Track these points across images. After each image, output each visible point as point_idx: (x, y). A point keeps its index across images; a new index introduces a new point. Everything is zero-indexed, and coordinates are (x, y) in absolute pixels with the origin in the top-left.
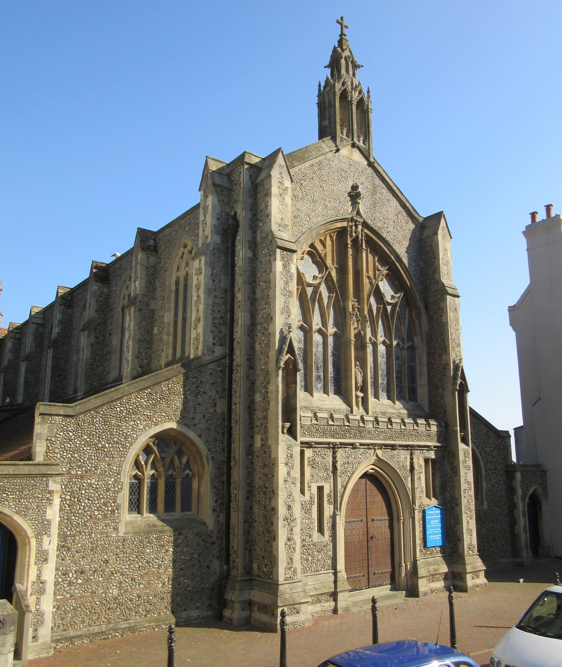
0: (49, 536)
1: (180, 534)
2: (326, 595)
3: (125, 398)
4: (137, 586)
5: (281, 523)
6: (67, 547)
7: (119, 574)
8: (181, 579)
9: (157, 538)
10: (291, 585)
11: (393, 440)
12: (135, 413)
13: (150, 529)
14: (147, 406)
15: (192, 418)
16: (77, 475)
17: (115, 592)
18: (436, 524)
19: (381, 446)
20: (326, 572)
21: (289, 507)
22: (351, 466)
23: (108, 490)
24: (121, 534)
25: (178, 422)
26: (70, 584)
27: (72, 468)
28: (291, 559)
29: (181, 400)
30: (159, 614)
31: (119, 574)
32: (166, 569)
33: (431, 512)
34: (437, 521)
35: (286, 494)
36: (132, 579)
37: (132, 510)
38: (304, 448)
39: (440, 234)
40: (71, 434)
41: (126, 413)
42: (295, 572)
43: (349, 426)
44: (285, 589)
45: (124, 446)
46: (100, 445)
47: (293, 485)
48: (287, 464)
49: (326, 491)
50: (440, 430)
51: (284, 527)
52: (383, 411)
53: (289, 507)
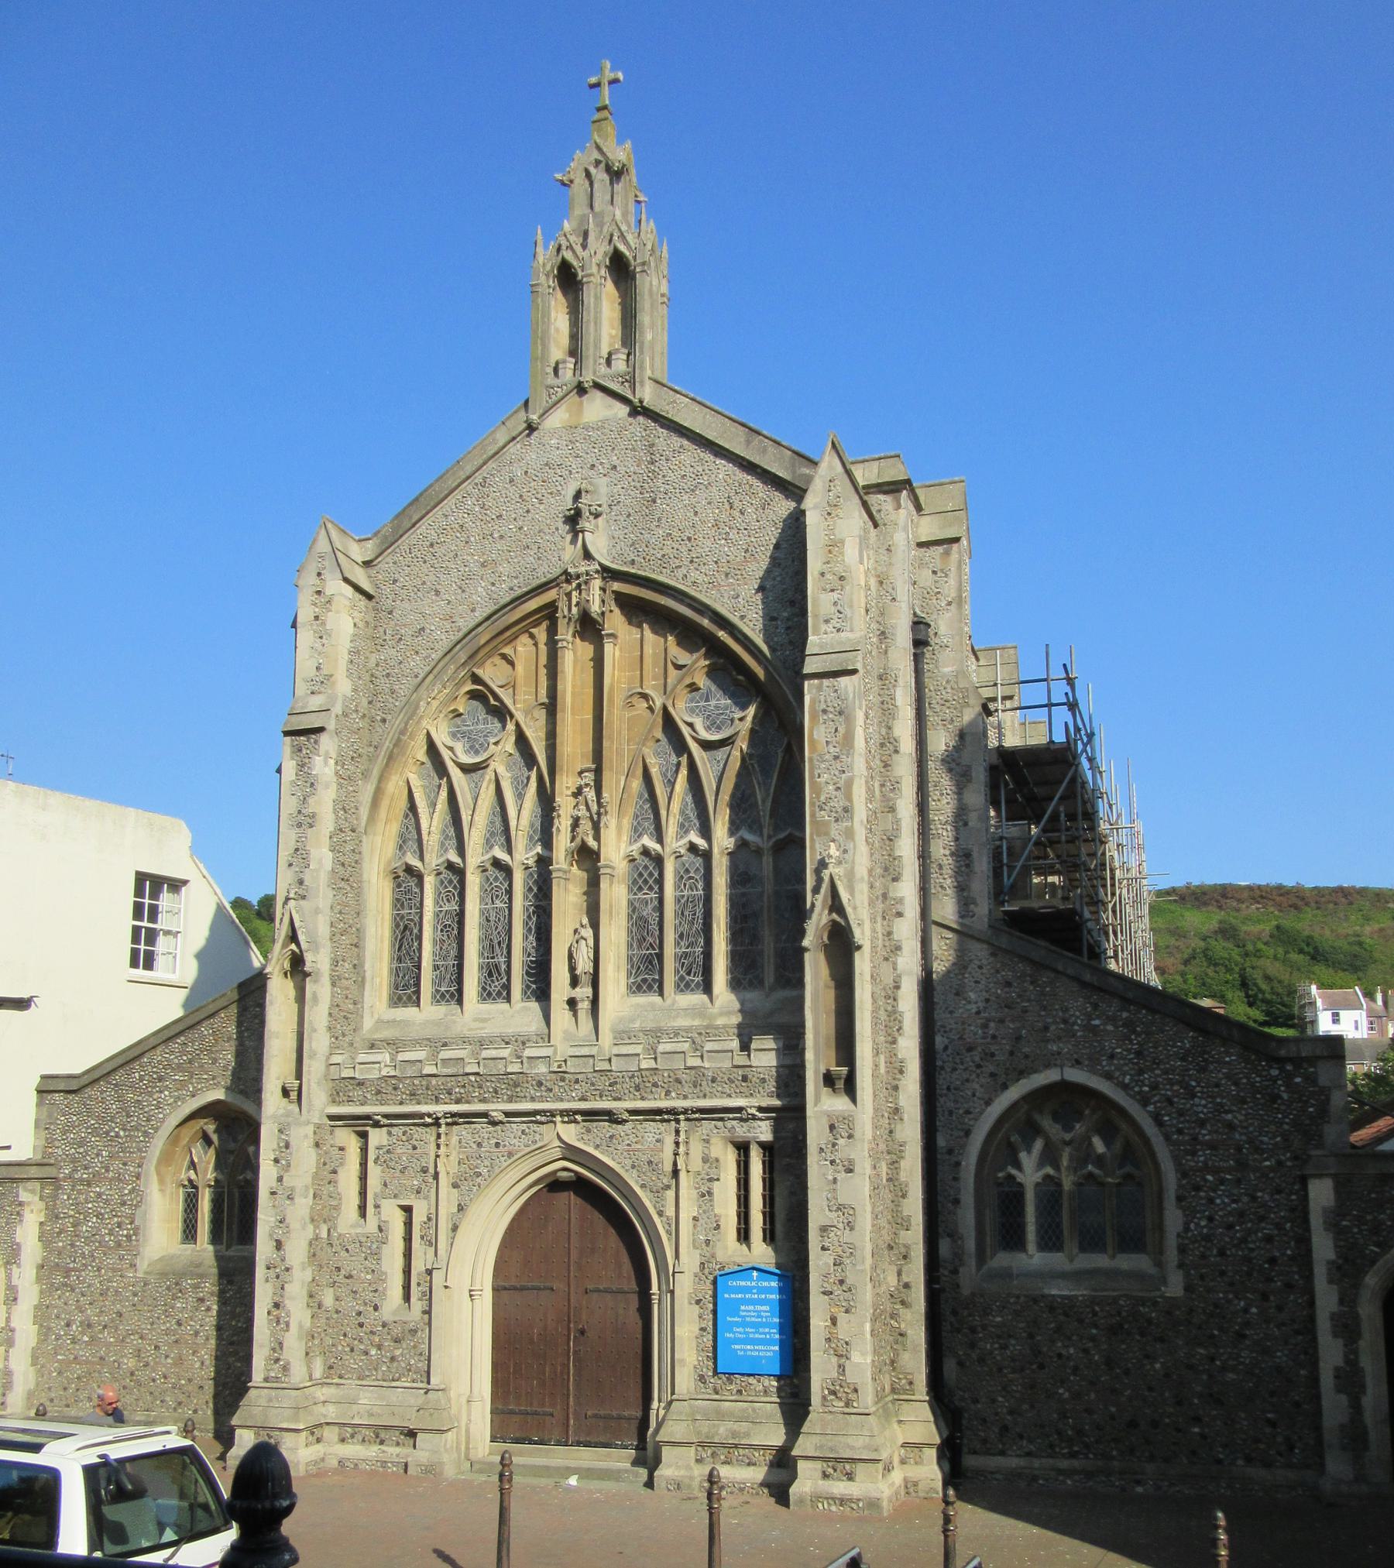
0: (19, 1266)
1: (230, 1282)
2: (397, 1433)
3: (147, 1055)
4: (163, 1360)
5: (260, 1272)
6: (71, 1286)
7: (137, 1336)
8: (231, 1360)
9: (196, 1287)
10: (273, 1393)
11: (615, 1100)
12: (160, 1079)
13: (193, 1270)
14: (179, 1065)
15: (253, 1079)
16: (81, 1180)
17: (130, 1363)
18: (762, 1317)
19: (570, 1115)
20: (415, 1385)
21: (279, 1245)
22: (487, 1163)
23: (124, 1204)
24: (140, 1274)
25: (227, 1089)
26: (74, 1341)
27: (75, 1170)
28: (281, 1344)
29: (233, 1049)
30: (195, 1411)
31: (137, 1336)
32: (207, 1339)
33: (743, 1283)
34: (764, 1308)
35: (273, 1219)
36: (156, 1347)
37: (187, 1237)
38: (368, 1128)
39: (815, 507)
40: (75, 1118)
41: (149, 1081)
42: (285, 1369)
43: (477, 1074)
44: (259, 1396)
45: (146, 1134)
46: (112, 1134)
47: (288, 1202)
48: (276, 1161)
49: (418, 1218)
50: (788, 1062)
51: (267, 1281)
52: (650, 1025)
53: (279, 1245)
